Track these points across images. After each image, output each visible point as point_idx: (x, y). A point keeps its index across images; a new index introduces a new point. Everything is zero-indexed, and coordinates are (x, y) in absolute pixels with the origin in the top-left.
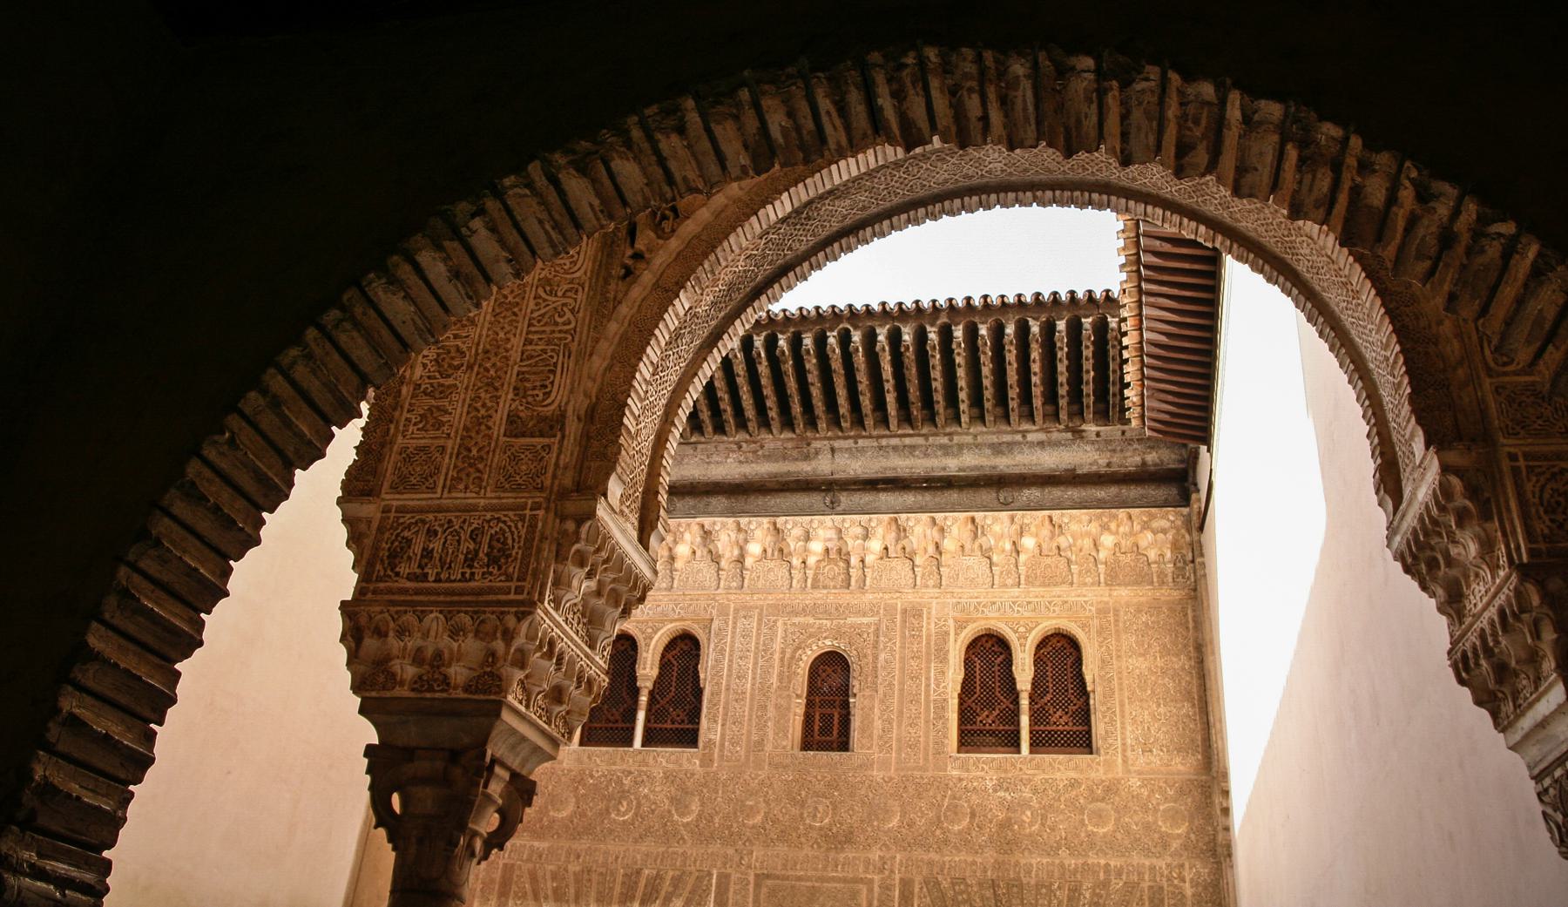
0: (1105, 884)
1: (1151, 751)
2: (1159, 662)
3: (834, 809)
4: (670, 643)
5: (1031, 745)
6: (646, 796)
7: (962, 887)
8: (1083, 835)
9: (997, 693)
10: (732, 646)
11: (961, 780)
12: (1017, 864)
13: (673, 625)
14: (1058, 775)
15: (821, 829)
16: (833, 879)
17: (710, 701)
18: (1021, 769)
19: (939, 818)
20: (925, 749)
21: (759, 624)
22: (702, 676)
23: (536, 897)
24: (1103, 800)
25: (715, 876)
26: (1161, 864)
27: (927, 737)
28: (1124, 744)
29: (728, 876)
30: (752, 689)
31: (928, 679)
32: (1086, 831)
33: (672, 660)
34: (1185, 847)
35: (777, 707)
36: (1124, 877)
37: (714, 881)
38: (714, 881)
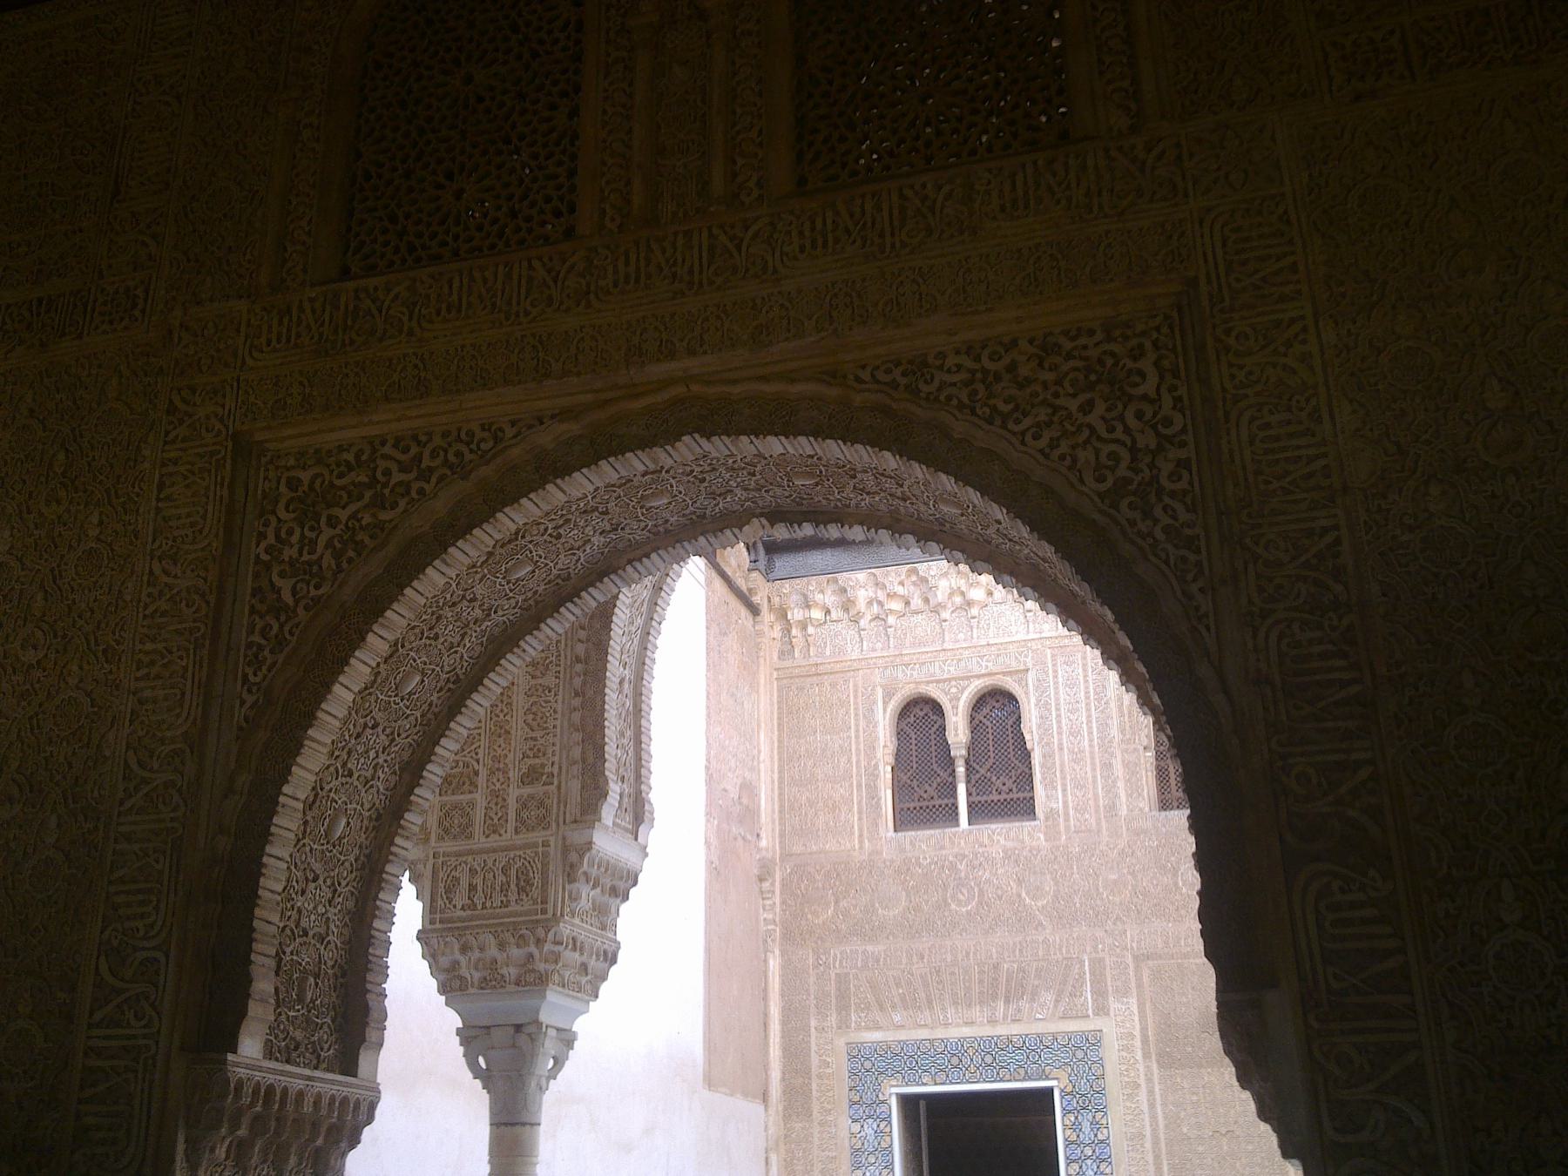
4: (977, 702)
6: (988, 881)
10: (1057, 699)
13: (981, 681)
17: (1043, 765)
21: (1085, 670)
22: (1027, 737)
23: (881, 1008)
25: (1087, 964)
29: (1101, 960)
30: (1091, 746)
33: (985, 721)
35: (1126, 765)
37: (1087, 968)
38: (1087, 968)
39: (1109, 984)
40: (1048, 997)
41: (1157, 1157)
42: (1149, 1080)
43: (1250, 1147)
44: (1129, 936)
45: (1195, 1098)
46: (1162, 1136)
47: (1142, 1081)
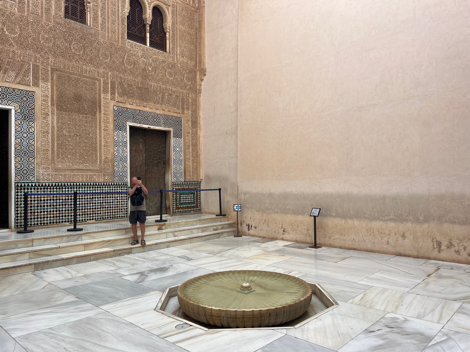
0: (171, 95)
1: (184, 57)
2: (187, 30)
3: (84, 48)
5: (150, 44)
7: (131, 88)
8: (166, 78)
9: (137, 22)
11: (130, 50)
12: (148, 84)
14: (159, 57)
15: (79, 55)
16: (84, 77)
18: (149, 52)
19: (123, 62)
20: (118, 35)
24: (171, 69)
25: (31, 65)
26: (185, 92)
27: (118, 30)
28: (177, 53)
31: (118, 7)
32: (167, 78)
34: (190, 88)
36: (176, 94)
37: (31, 67)
38: (31, 67)
39: (40, 75)
40: (13, 74)
41: (53, 140)
42: (53, 114)
43: (86, 141)
44: (50, 60)
45: (69, 122)
46: (55, 133)
47: (50, 113)
